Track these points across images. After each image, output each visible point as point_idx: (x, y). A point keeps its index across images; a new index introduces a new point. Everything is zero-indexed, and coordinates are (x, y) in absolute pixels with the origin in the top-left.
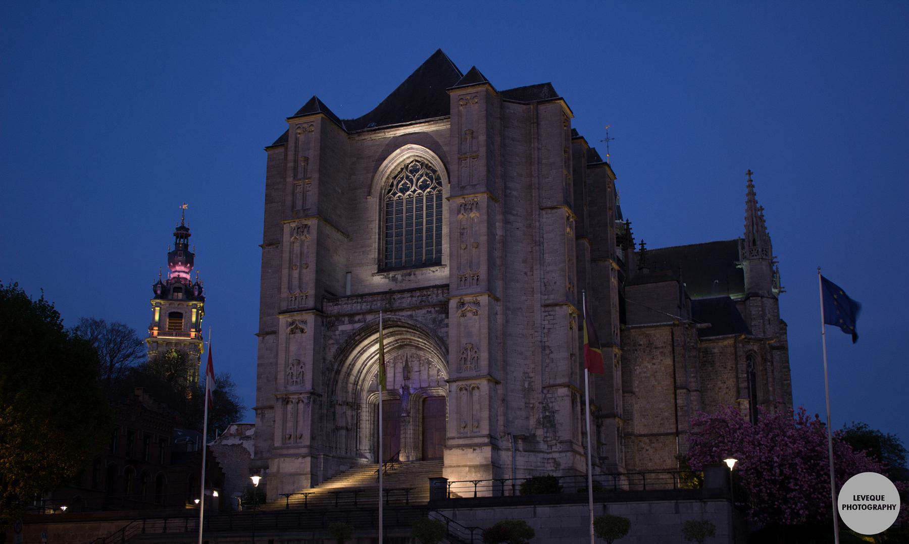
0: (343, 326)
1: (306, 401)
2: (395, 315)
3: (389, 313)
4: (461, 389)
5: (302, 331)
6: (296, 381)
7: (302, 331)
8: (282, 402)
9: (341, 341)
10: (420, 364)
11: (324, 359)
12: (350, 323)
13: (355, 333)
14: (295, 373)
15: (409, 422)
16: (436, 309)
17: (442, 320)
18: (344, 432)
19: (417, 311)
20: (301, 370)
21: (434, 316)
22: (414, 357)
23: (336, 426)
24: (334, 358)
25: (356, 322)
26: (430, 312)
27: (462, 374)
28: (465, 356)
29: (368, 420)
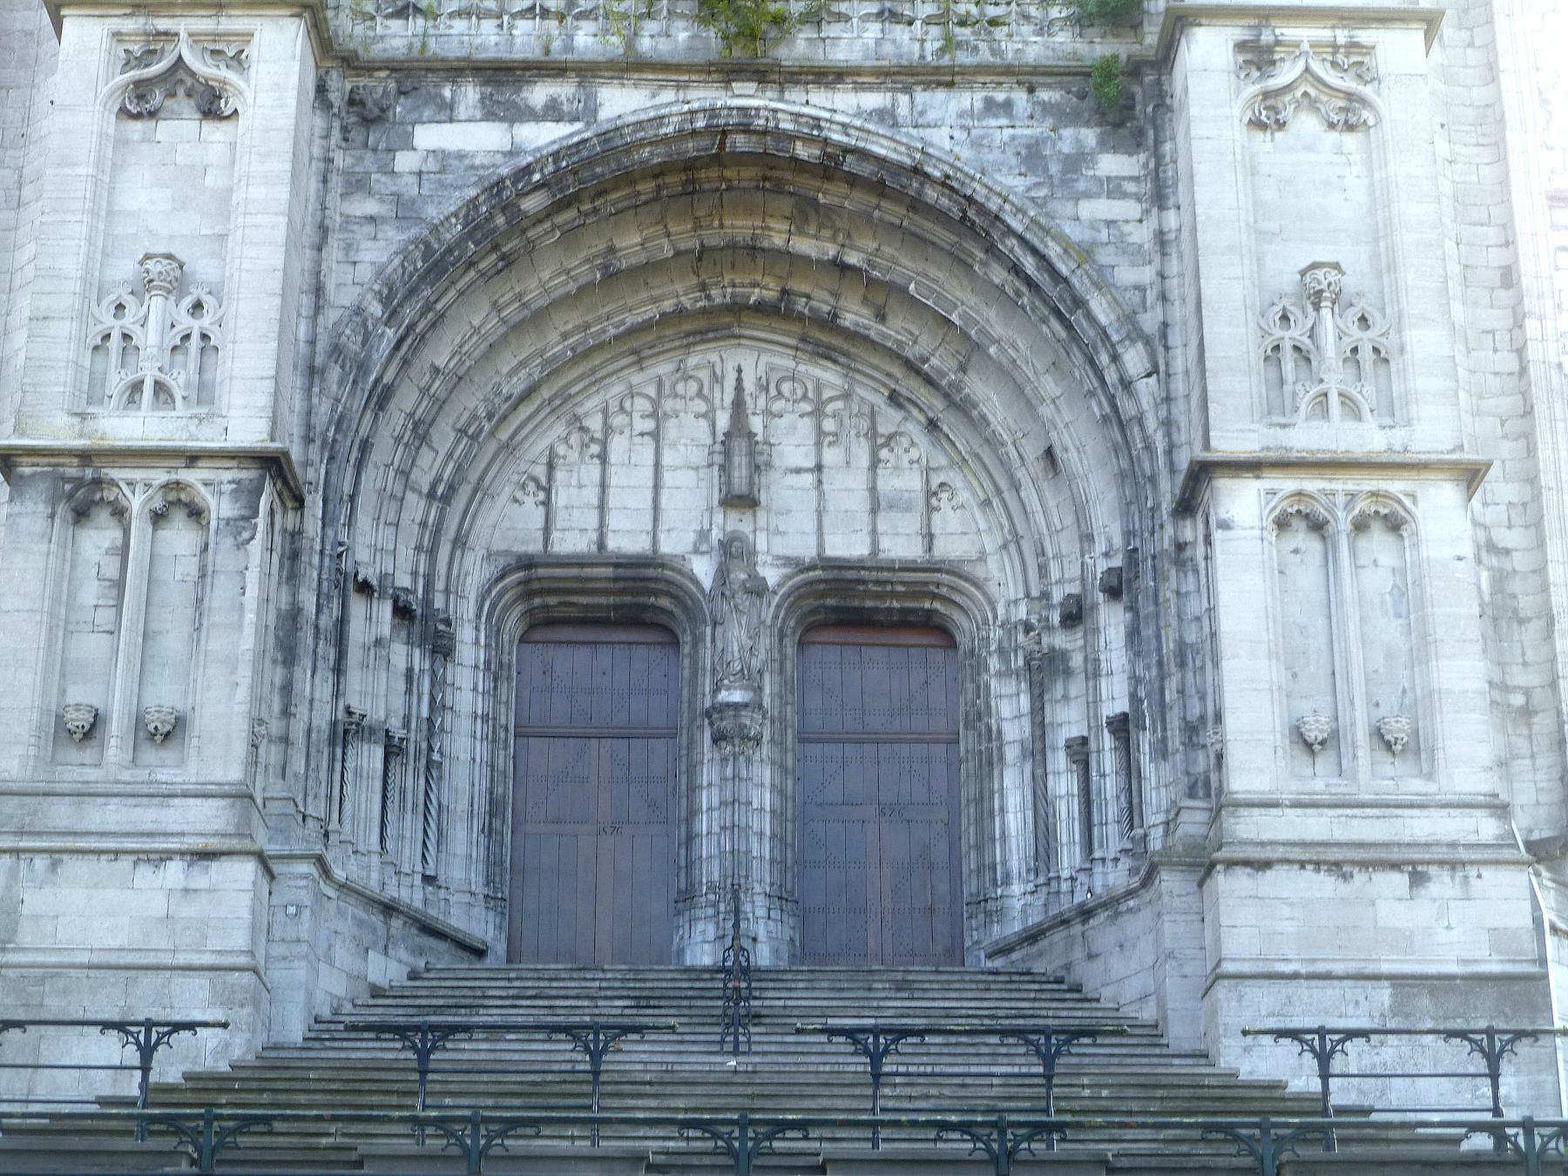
0: (447, 126)
1: (221, 508)
2: (781, 100)
3: (751, 87)
4: (1282, 524)
5: (212, 106)
6: (159, 386)
7: (212, 106)
8: (53, 502)
9: (433, 212)
10: (820, 433)
11: (318, 290)
12: (489, 116)
13: (527, 170)
14: (151, 339)
15: (758, 741)
16: (1044, 95)
17: (1076, 162)
18: (370, 757)
19: (921, 96)
20: (196, 325)
21: (1027, 132)
22: (780, 394)
23: (349, 713)
24: (385, 301)
25: (527, 114)
26: (1008, 106)
27: (1291, 432)
28: (1297, 333)
29: (485, 718)
